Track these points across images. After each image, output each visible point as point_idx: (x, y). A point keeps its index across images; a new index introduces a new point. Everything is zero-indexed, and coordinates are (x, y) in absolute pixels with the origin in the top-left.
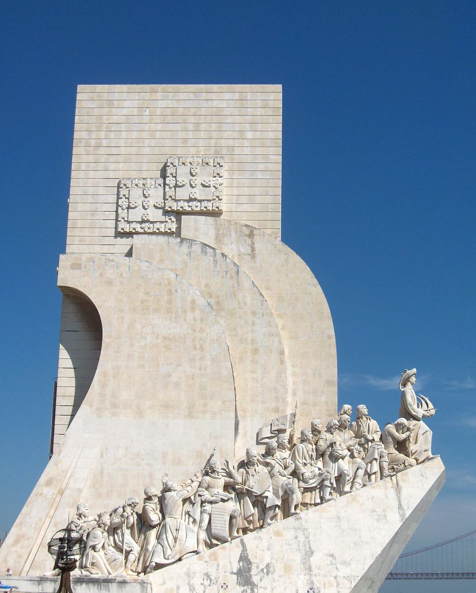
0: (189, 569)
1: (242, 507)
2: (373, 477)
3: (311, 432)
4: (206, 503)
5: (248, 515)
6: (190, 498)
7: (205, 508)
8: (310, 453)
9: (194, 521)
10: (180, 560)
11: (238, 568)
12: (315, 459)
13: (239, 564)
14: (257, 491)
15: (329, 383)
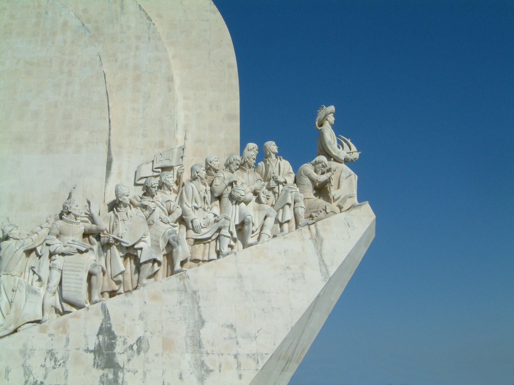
0: (25, 345)
1: (108, 262)
2: (286, 226)
3: (203, 168)
4: (57, 255)
5: (117, 273)
6: (34, 249)
7: (55, 262)
8: (203, 194)
9: (40, 280)
10: (15, 331)
11: (97, 343)
12: (209, 203)
13: (98, 338)
14: (128, 241)
15: (230, 117)
